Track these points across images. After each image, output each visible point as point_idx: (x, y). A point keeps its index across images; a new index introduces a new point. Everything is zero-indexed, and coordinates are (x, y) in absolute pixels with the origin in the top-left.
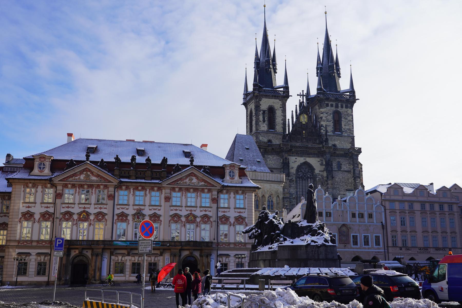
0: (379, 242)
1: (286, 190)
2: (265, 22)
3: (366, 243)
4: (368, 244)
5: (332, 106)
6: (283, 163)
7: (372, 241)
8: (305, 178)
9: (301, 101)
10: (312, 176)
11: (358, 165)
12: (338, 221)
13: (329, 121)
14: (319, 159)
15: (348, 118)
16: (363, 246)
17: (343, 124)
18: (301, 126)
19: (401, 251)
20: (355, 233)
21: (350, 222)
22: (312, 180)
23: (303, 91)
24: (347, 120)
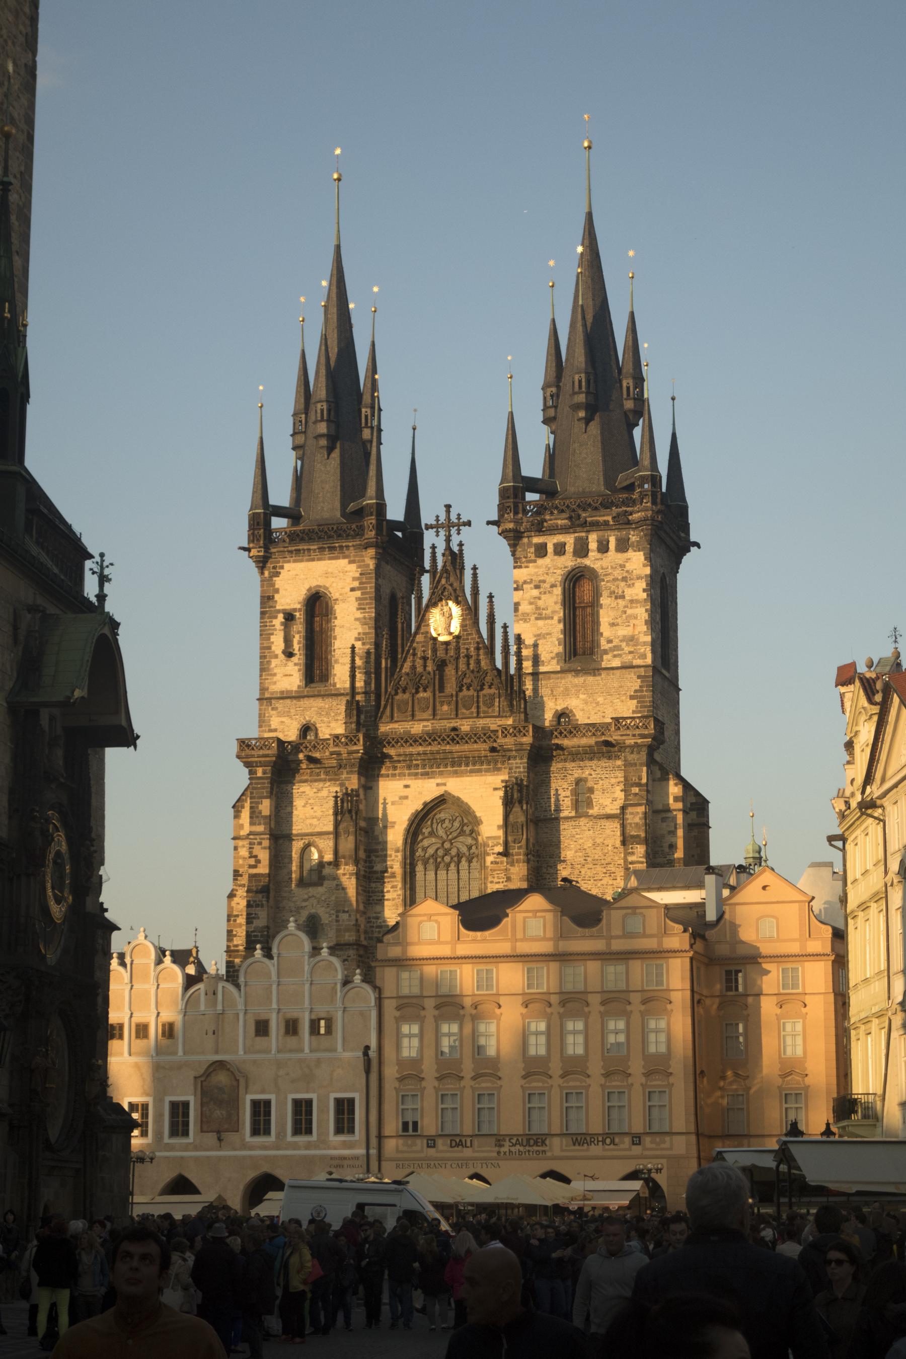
1: (344, 916)
2: (338, 248)
4: (309, 1131)
5: (560, 550)
6: (336, 814)
7: (324, 1118)
8: (447, 859)
9: (440, 551)
13: (546, 618)
14: (498, 779)
15: (630, 593)
16: (290, 1138)
17: (605, 617)
18: (435, 650)
19: (432, 1151)
20: (263, 1092)
22: (474, 864)
23: (448, 507)
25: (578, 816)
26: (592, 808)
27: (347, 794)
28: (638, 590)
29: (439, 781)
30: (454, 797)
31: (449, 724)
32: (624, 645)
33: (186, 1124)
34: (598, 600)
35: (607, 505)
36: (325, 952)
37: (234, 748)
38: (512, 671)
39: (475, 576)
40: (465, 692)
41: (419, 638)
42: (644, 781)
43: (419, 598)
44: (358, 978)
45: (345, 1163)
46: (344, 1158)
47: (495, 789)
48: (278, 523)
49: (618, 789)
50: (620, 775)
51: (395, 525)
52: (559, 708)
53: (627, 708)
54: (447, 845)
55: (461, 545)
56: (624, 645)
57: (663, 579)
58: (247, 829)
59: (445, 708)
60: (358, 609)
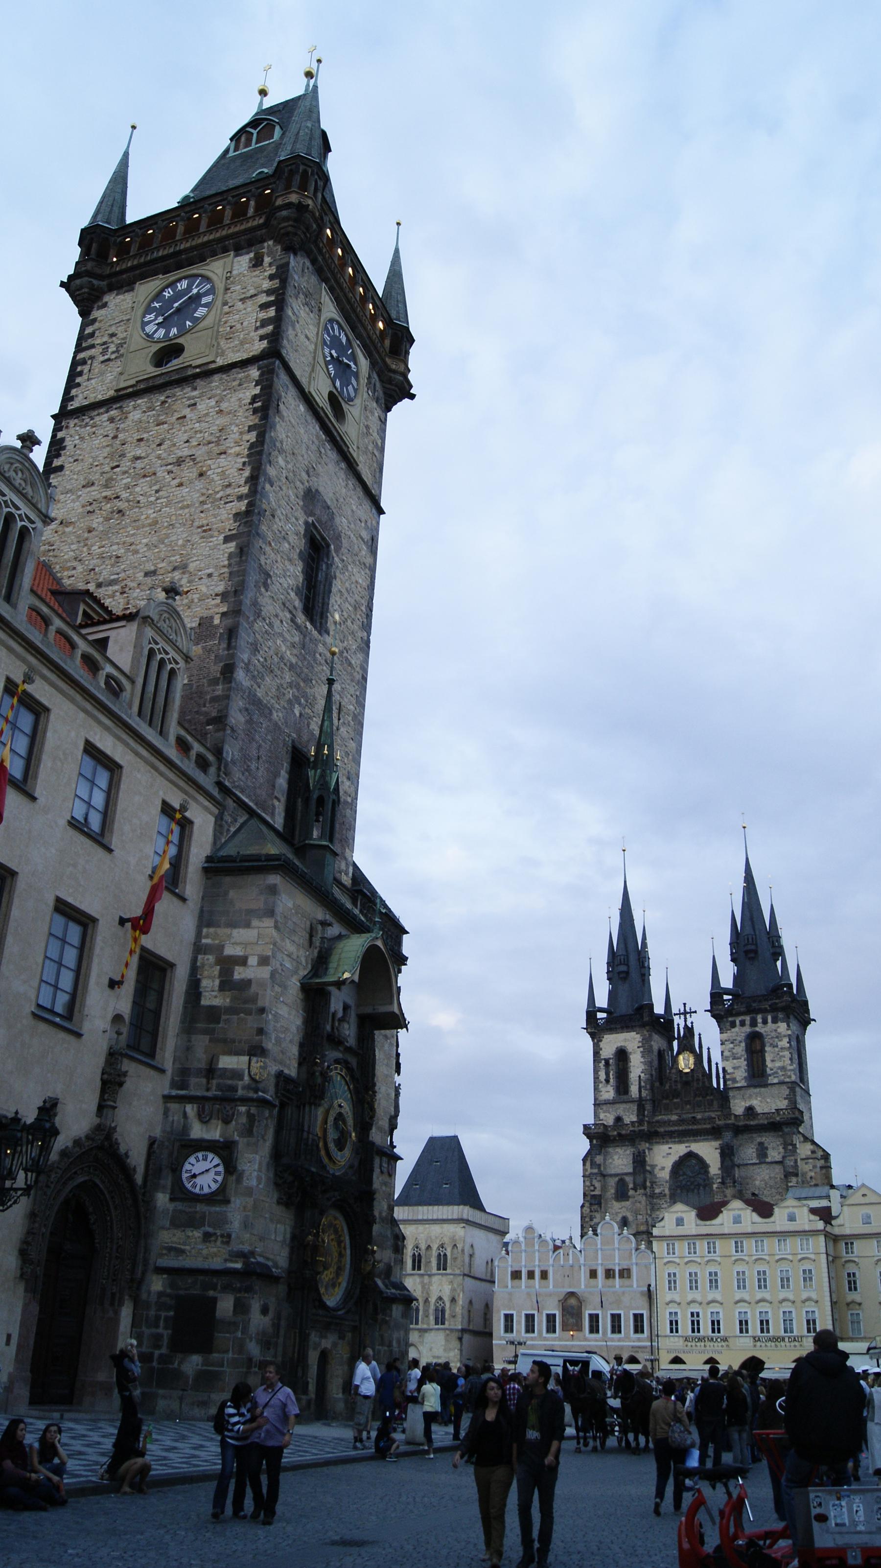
0: (642, 1326)
1: (640, 1217)
2: (625, 882)
3: (616, 1327)
4: (620, 1332)
5: (743, 1024)
6: (633, 1163)
7: (628, 1324)
8: (692, 1187)
10: (707, 1182)
11: (794, 1146)
12: (563, 1287)
14: (716, 1144)
15: (780, 1044)
17: (768, 1058)
18: (681, 1077)
20: (595, 1309)
21: (586, 1286)
23: (685, 1004)
24: (776, 1049)
25: (760, 1163)
27: (639, 1152)
28: (784, 1043)
31: (690, 1116)
33: (555, 1326)
35: (766, 1000)
36: (625, 1232)
37: (582, 1129)
38: (722, 1086)
39: (700, 1038)
40: (698, 1099)
41: (674, 1071)
43: (672, 1050)
44: (643, 1247)
45: (640, 1350)
46: (639, 1347)
48: (600, 1015)
49: (781, 1147)
51: (659, 1016)
53: (783, 1104)
54: (692, 1180)
55: (692, 1023)
57: (798, 1037)
58: (589, 1171)
59: (688, 1106)
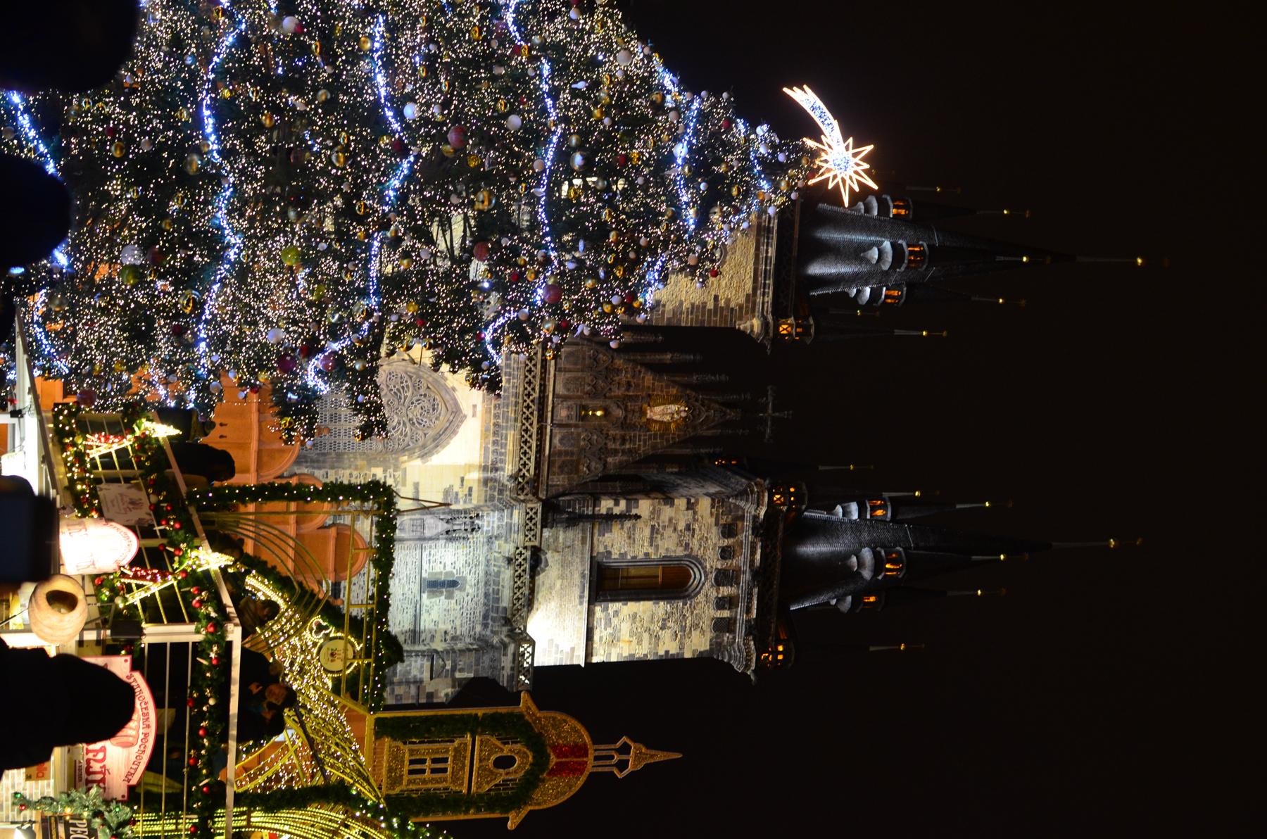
5: (726, 553)
15: (666, 635)
17: (643, 608)
26: (429, 597)
29: (479, 409)
30: (458, 427)
32: (610, 630)
34: (662, 599)
42: (458, 675)
47: (462, 479)
49: (448, 627)
50: (463, 630)
52: (549, 555)
56: (610, 630)
59: (564, 413)
60: (693, 305)
